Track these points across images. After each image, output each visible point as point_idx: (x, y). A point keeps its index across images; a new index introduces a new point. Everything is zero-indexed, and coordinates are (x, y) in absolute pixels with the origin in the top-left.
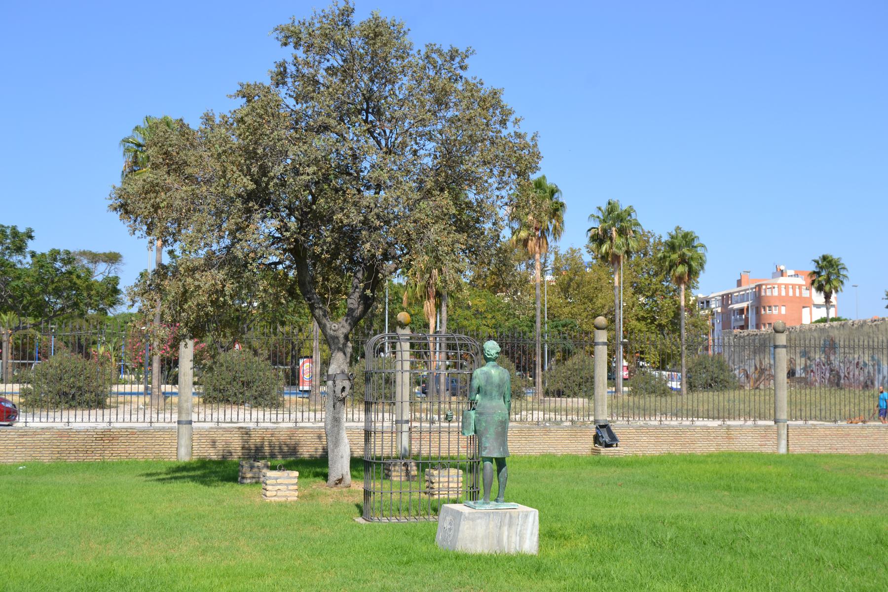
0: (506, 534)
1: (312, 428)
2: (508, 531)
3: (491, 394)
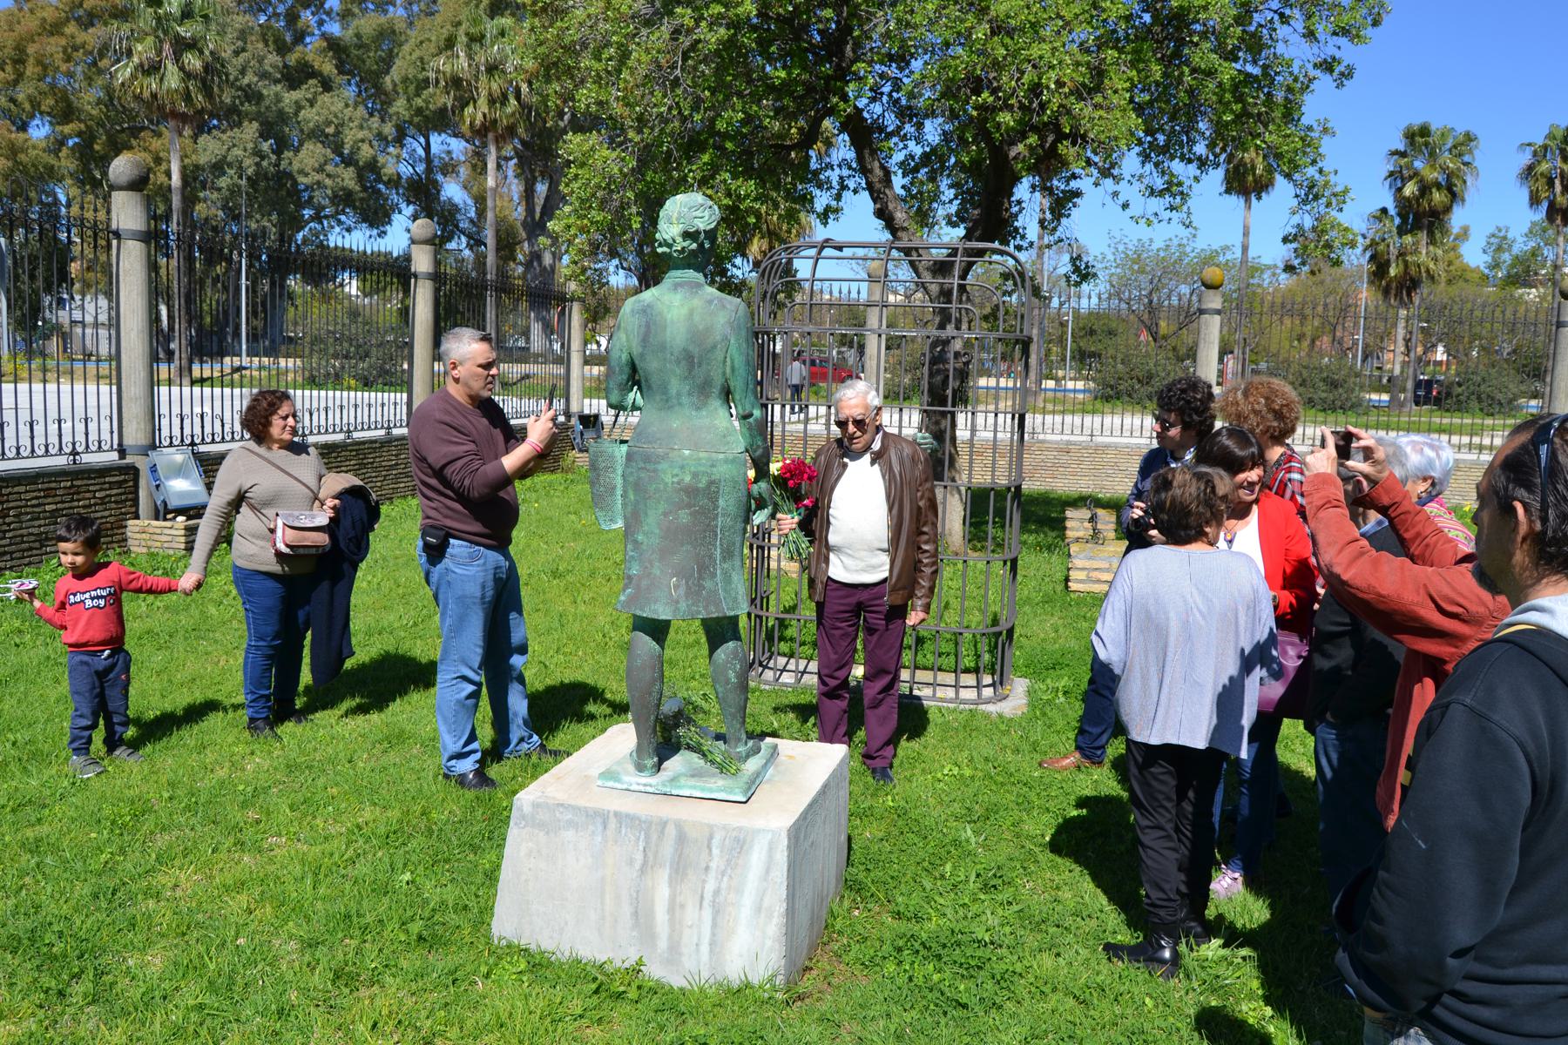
0: (662, 893)
1: (1057, 442)
2: (671, 882)
3: (664, 389)
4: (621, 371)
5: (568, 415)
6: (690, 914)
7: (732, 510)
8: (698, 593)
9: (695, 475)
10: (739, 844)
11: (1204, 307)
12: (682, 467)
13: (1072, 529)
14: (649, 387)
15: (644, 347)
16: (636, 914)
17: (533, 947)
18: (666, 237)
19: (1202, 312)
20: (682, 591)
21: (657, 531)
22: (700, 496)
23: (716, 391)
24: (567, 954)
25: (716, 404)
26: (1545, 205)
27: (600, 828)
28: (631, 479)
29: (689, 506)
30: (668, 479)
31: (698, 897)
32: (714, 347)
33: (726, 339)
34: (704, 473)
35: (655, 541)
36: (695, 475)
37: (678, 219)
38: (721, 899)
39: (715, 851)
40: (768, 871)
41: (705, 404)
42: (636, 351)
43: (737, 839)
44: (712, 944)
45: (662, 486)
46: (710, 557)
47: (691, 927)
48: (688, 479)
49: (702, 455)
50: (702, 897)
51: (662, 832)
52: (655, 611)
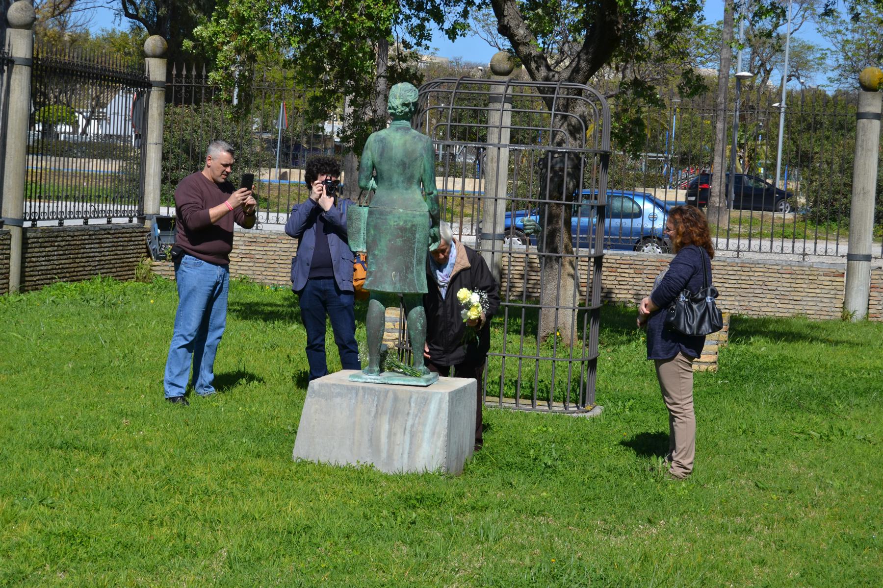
0: (385, 427)
2: (390, 422)
3: (390, 179)
4: (367, 170)
5: (142, 218)
6: (399, 438)
7: (422, 240)
9: (405, 222)
10: (425, 401)
11: (862, 110)
12: (399, 218)
14: (382, 178)
16: (371, 440)
17: (316, 461)
18: (394, 105)
19: (860, 116)
20: (398, 278)
21: (385, 249)
22: (407, 232)
23: (416, 181)
24: (333, 464)
27: (354, 395)
28: (372, 223)
29: (402, 237)
30: (392, 223)
31: (403, 429)
32: (416, 159)
33: (422, 155)
34: (409, 221)
36: (405, 222)
37: (400, 97)
38: (415, 429)
39: (413, 405)
40: (438, 413)
41: (410, 187)
42: (377, 159)
43: (424, 398)
45: (388, 227)
46: (411, 263)
47: (399, 445)
49: (409, 212)
50: (405, 429)
51: (386, 396)
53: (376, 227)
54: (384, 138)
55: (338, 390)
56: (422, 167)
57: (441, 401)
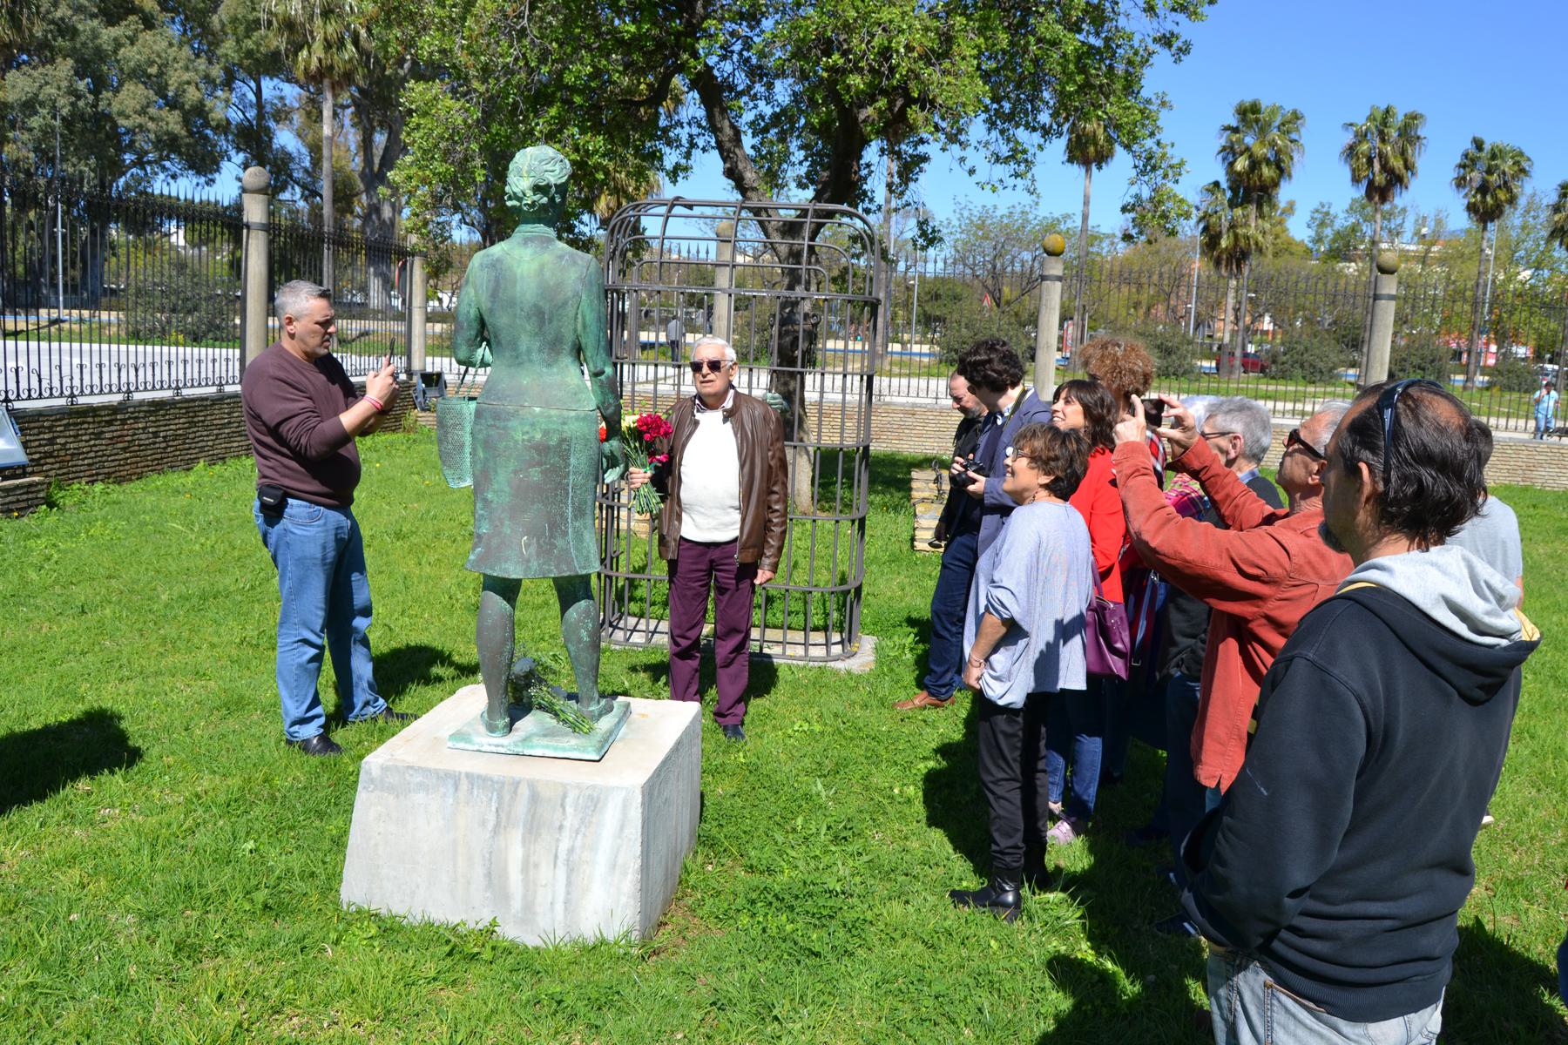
0: (516, 853)
1: (903, 405)
3: (514, 345)
5: (409, 373)
6: (545, 872)
7: (584, 468)
8: (549, 552)
9: (546, 433)
10: (593, 802)
11: (1046, 273)
12: (533, 425)
13: (918, 490)
14: (499, 343)
15: (493, 302)
16: (489, 875)
17: (384, 912)
18: (516, 190)
19: (1043, 278)
20: (533, 549)
21: (507, 489)
22: (552, 454)
23: (567, 347)
24: (419, 917)
25: (567, 361)
26: (1365, 183)
27: (451, 790)
28: (480, 436)
29: (540, 464)
30: (519, 436)
31: (552, 857)
32: (565, 303)
33: (577, 295)
35: (505, 499)
36: (546, 433)
37: (528, 172)
38: (575, 857)
39: (569, 810)
40: (622, 828)
41: (556, 361)
42: (486, 305)
43: (591, 798)
44: (567, 902)
46: (562, 516)
47: (545, 886)
48: (538, 436)
49: (553, 412)
50: (556, 857)
51: (515, 792)
52: (505, 570)
53: (487, 444)
54: (498, 260)
55: (419, 779)
56: (580, 320)
57: (625, 806)
